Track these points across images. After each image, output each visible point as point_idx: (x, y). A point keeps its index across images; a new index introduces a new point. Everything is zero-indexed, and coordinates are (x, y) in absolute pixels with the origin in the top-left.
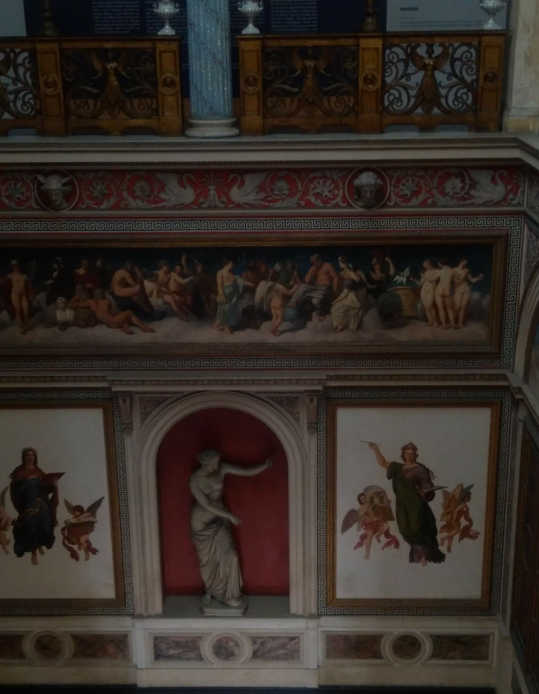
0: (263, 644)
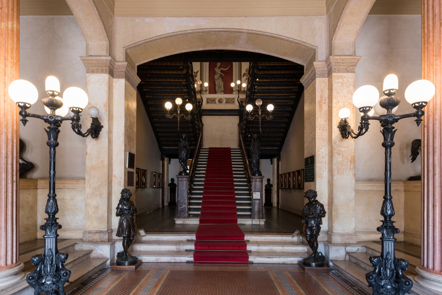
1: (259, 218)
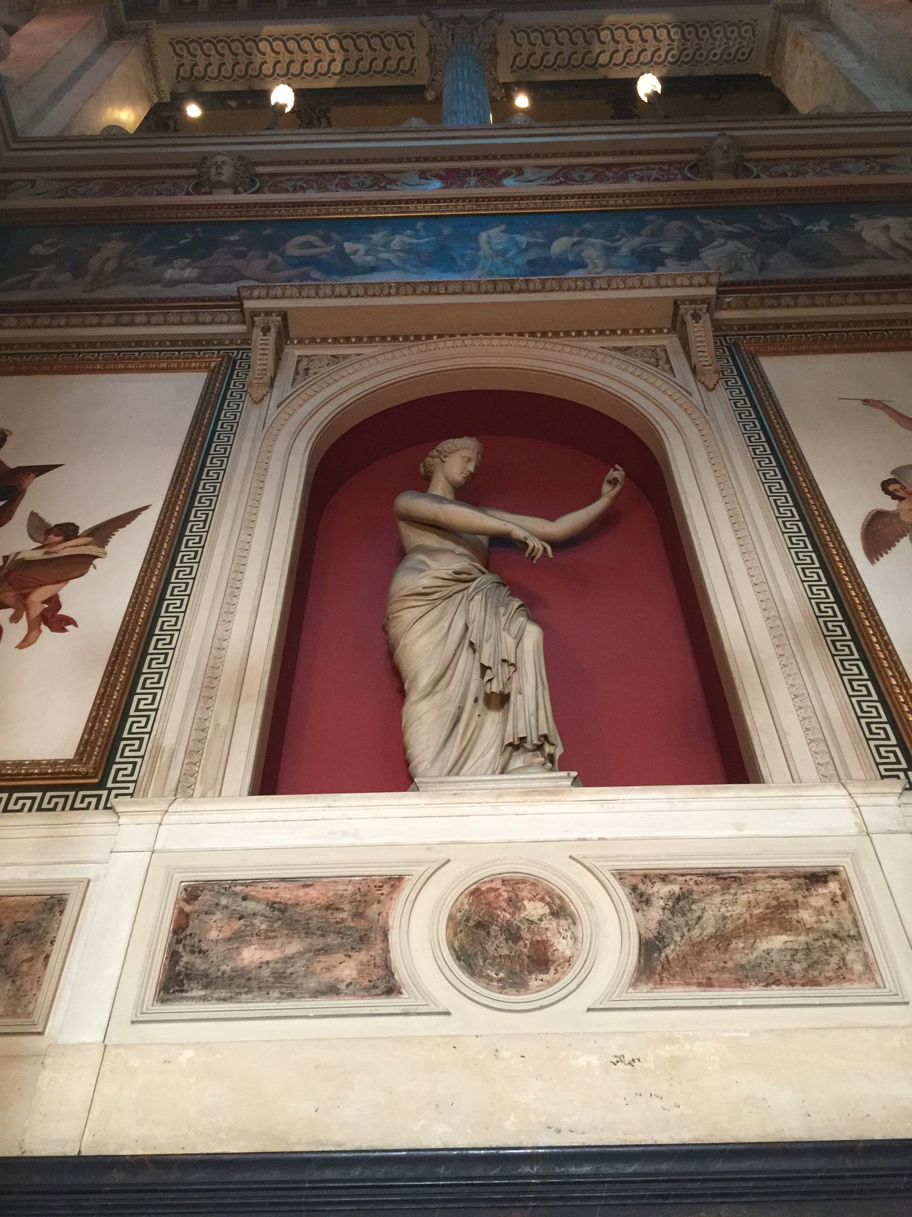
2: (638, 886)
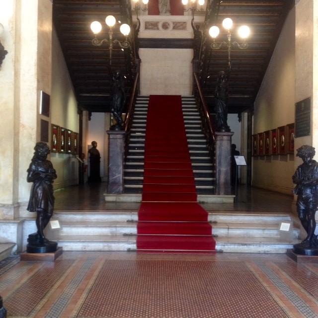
0: (176, 24)
1: (226, 193)
2: (174, 23)
